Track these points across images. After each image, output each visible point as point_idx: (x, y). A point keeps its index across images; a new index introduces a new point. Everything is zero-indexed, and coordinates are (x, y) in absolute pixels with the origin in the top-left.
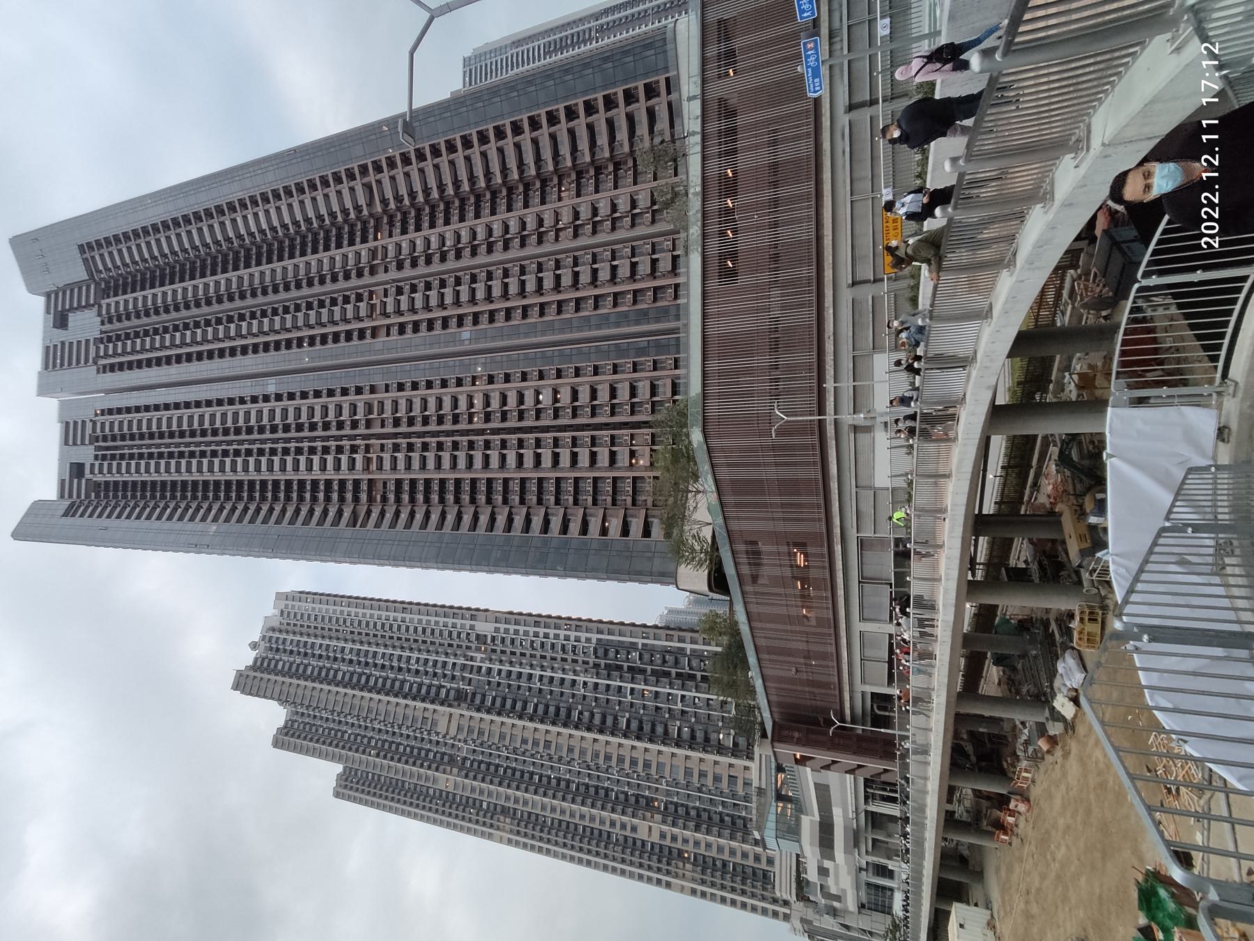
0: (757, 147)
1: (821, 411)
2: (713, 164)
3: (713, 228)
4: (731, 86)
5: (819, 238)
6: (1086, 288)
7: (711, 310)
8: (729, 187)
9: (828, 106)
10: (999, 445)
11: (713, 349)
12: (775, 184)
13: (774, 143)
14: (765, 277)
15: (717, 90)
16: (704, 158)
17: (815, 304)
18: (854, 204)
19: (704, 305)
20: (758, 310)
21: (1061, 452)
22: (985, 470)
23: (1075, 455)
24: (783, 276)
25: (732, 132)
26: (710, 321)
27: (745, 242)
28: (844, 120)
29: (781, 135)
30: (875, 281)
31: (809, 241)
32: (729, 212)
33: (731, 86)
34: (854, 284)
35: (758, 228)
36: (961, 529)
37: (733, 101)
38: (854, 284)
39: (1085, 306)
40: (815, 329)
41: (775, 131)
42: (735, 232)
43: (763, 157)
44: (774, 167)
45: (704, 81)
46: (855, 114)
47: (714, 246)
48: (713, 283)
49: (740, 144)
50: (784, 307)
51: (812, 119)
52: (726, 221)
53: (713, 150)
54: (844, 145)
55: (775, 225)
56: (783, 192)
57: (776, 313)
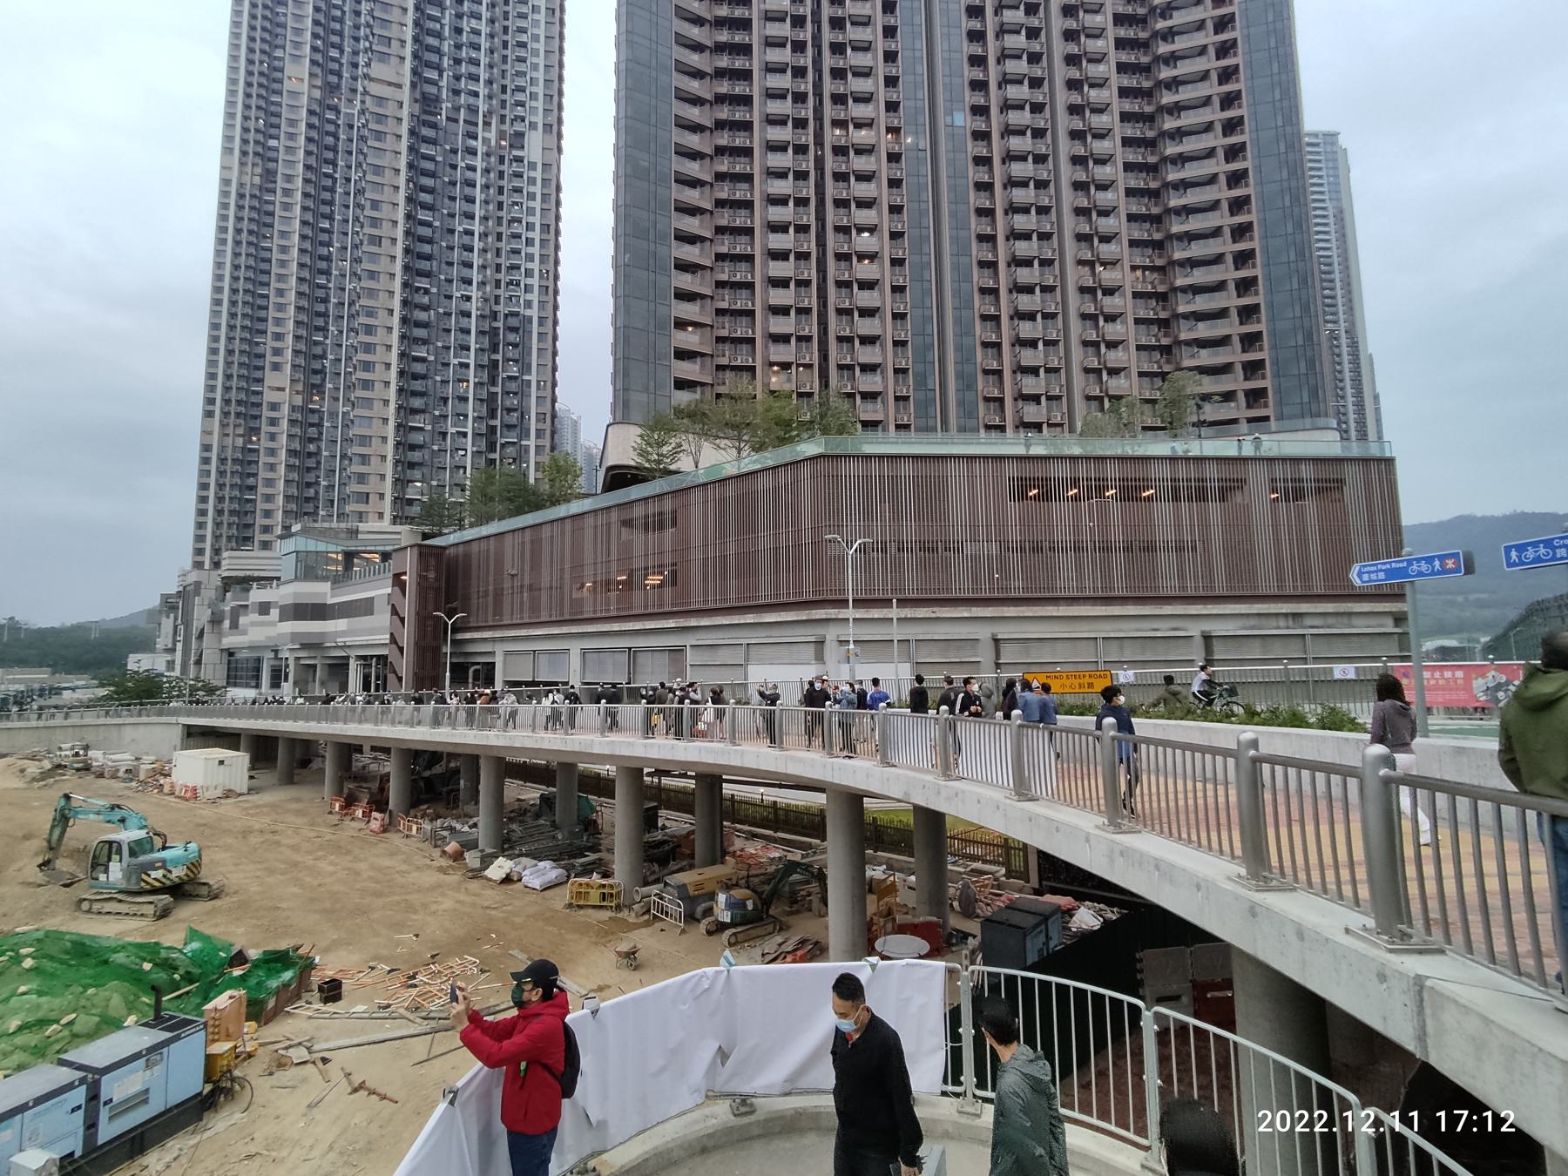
0: (1178, 526)
1: (858, 603)
2: (1164, 471)
3: (1082, 471)
4: (1258, 492)
5: (1054, 601)
6: (985, 886)
7: (978, 467)
8: (1130, 492)
9: (1215, 612)
10: (820, 799)
11: (927, 469)
12: (1128, 549)
13: (1180, 549)
14: (1014, 535)
15: (1257, 478)
16: (1173, 459)
17: (976, 596)
18: (1092, 643)
19: (985, 458)
20: (974, 527)
21: (798, 864)
22: (780, 786)
23: (795, 877)
24: (1014, 559)
25: (1202, 495)
26: (963, 466)
27: (1061, 511)
28: (1195, 630)
29: (1188, 555)
30: (998, 665)
31: (1054, 589)
32: (1101, 491)
33: (1258, 492)
34: (996, 641)
35: (1077, 527)
36: (711, 761)
37: (1238, 498)
38: (996, 641)
39: (966, 886)
40: (945, 596)
41: (1194, 549)
42: (1075, 498)
43: (1164, 532)
44: (1150, 548)
45: (1271, 460)
46: (1199, 644)
47: (1060, 471)
48: (1012, 470)
49: (1184, 505)
50: (975, 558)
51: (1202, 593)
52: (1090, 488)
53: (1182, 471)
54: (1164, 629)
55: (1078, 549)
56: (1118, 559)
57: (968, 549)
